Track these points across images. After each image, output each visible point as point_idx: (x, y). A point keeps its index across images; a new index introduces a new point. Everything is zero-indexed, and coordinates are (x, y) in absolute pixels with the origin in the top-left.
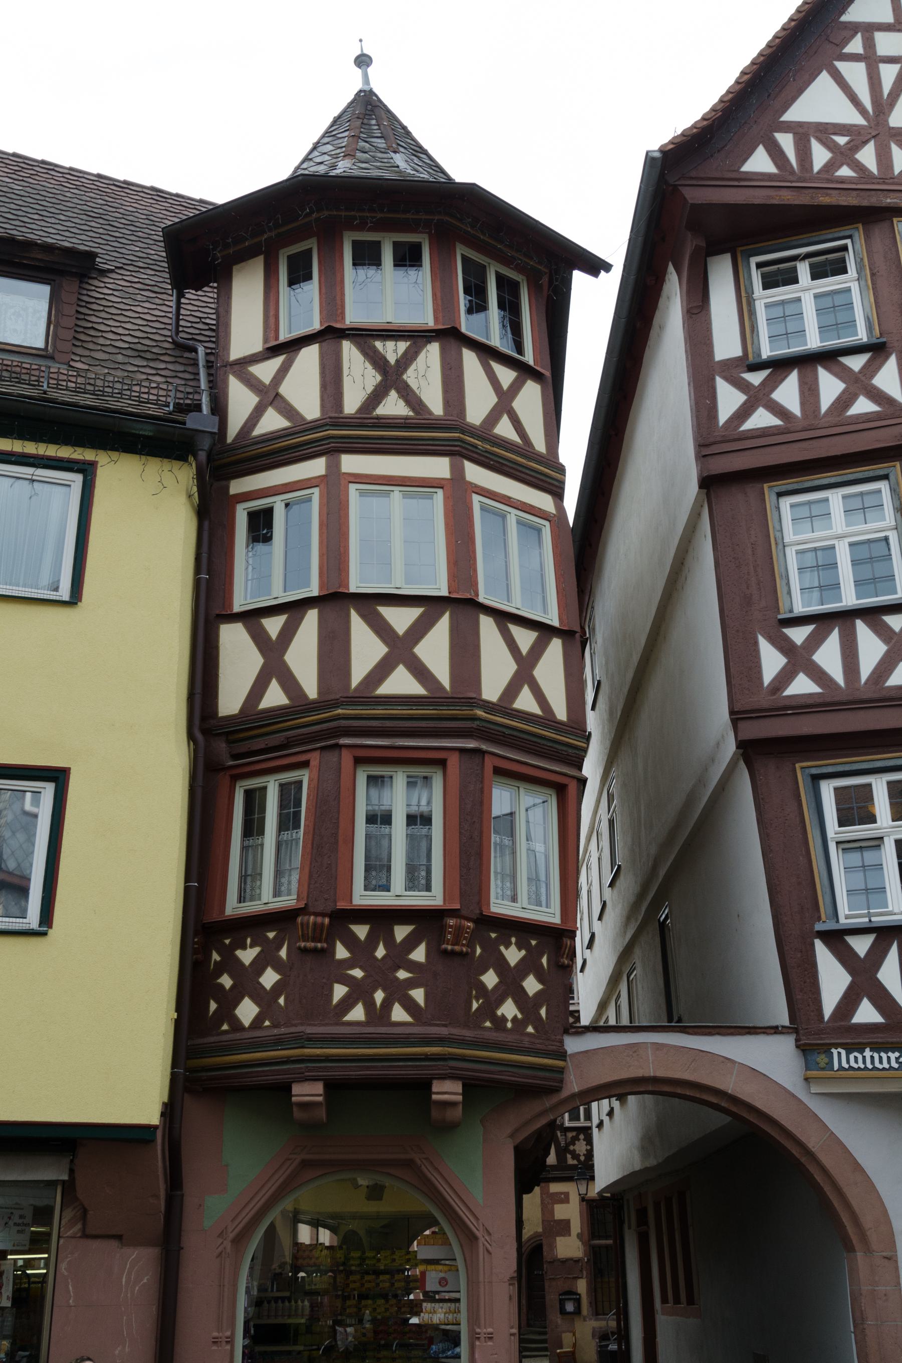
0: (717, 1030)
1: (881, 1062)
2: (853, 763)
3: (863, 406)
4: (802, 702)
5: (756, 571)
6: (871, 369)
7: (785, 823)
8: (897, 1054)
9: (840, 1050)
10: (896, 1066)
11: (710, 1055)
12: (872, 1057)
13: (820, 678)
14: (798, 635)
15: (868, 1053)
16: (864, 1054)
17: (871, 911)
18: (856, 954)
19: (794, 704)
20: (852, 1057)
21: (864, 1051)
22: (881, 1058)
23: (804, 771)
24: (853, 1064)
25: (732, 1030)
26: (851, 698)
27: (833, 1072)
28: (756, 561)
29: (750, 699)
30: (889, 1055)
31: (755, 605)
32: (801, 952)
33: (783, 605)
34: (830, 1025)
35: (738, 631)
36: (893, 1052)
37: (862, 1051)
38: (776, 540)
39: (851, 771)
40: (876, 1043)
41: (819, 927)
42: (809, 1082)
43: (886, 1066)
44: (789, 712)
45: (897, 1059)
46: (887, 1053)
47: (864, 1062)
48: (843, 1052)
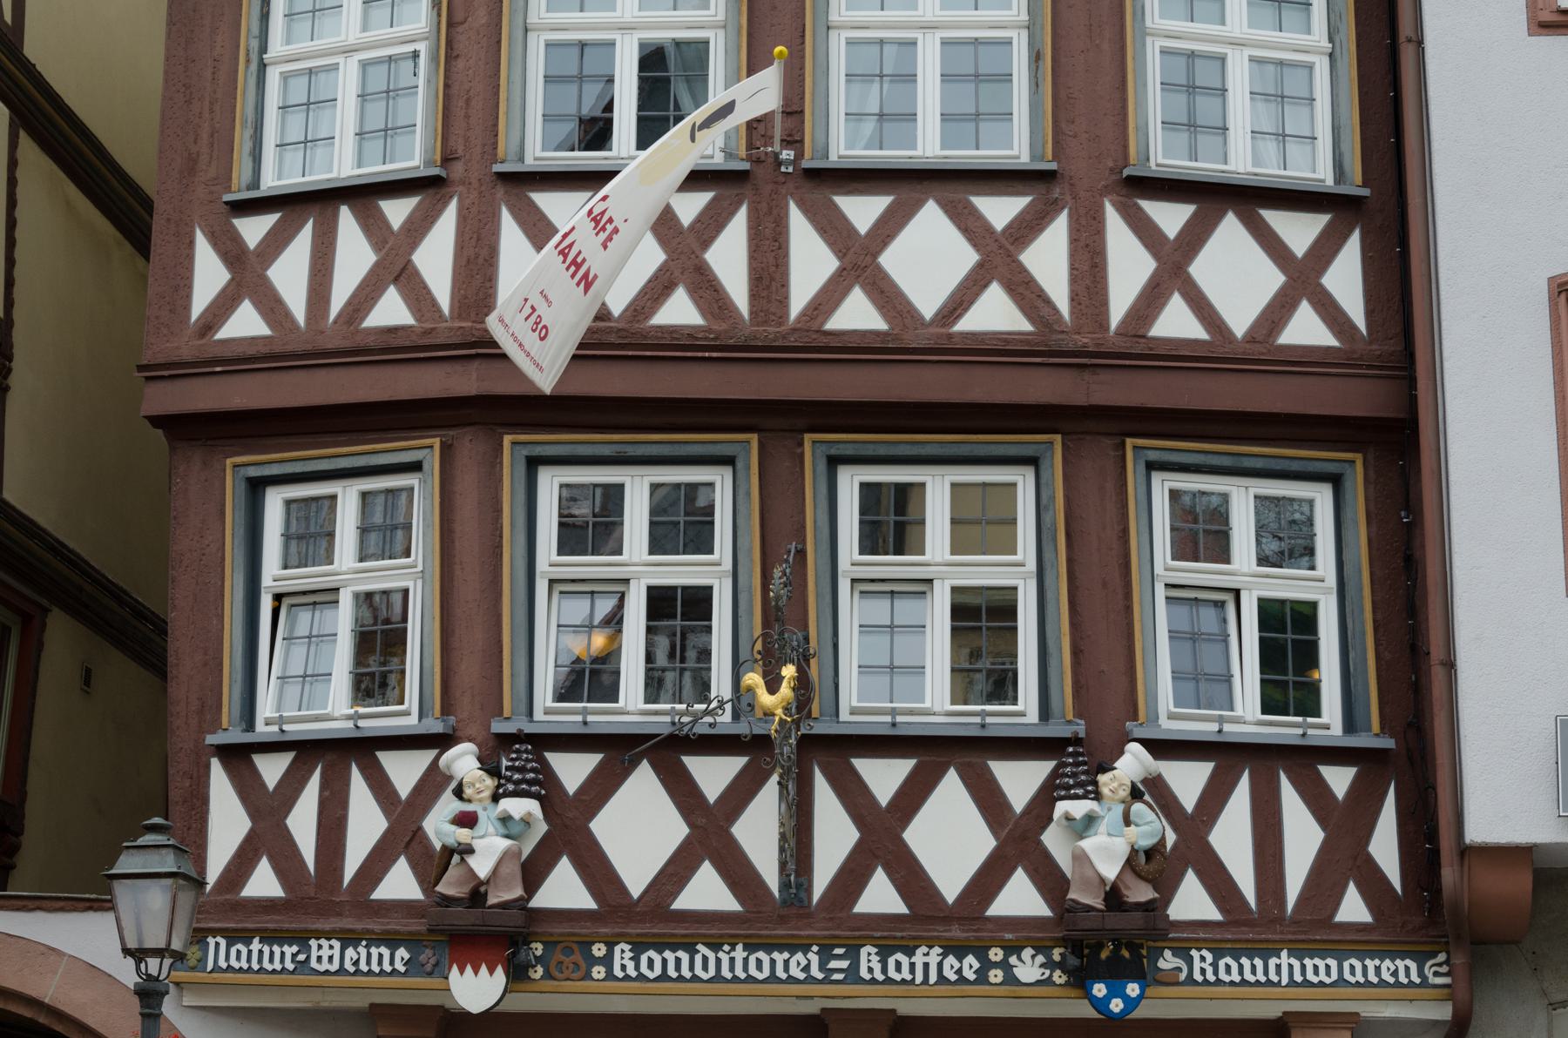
0: (37, 903)
1: (271, 960)
2: (333, 457)
4: (239, 351)
5: (212, 111)
7: (201, 560)
8: (295, 949)
9: (219, 939)
10: (290, 966)
11: (24, 942)
12: (261, 952)
13: (272, 309)
14: (253, 230)
15: (256, 945)
16: (251, 948)
17: (285, 714)
18: (263, 785)
19: (228, 354)
20: (233, 951)
21: (251, 943)
22: (272, 953)
23: (238, 472)
24: (234, 963)
25: (61, 904)
26: (309, 347)
27: (205, 975)
28: (215, 92)
29: (168, 345)
30: (283, 949)
31: (201, 174)
32: (191, 778)
33: (241, 171)
34: (212, 898)
35: (169, 220)
36: (290, 946)
37: (248, 942)
38: (248, 55)
39: (303, 473)
40: (266, 930)
41: (212, 739)
42: (182, 989)
43: (278, 967)
44: (218, 369)
45: (294, 956)
46: (281, 946)
47: (249, 960)
48: (223, 942)
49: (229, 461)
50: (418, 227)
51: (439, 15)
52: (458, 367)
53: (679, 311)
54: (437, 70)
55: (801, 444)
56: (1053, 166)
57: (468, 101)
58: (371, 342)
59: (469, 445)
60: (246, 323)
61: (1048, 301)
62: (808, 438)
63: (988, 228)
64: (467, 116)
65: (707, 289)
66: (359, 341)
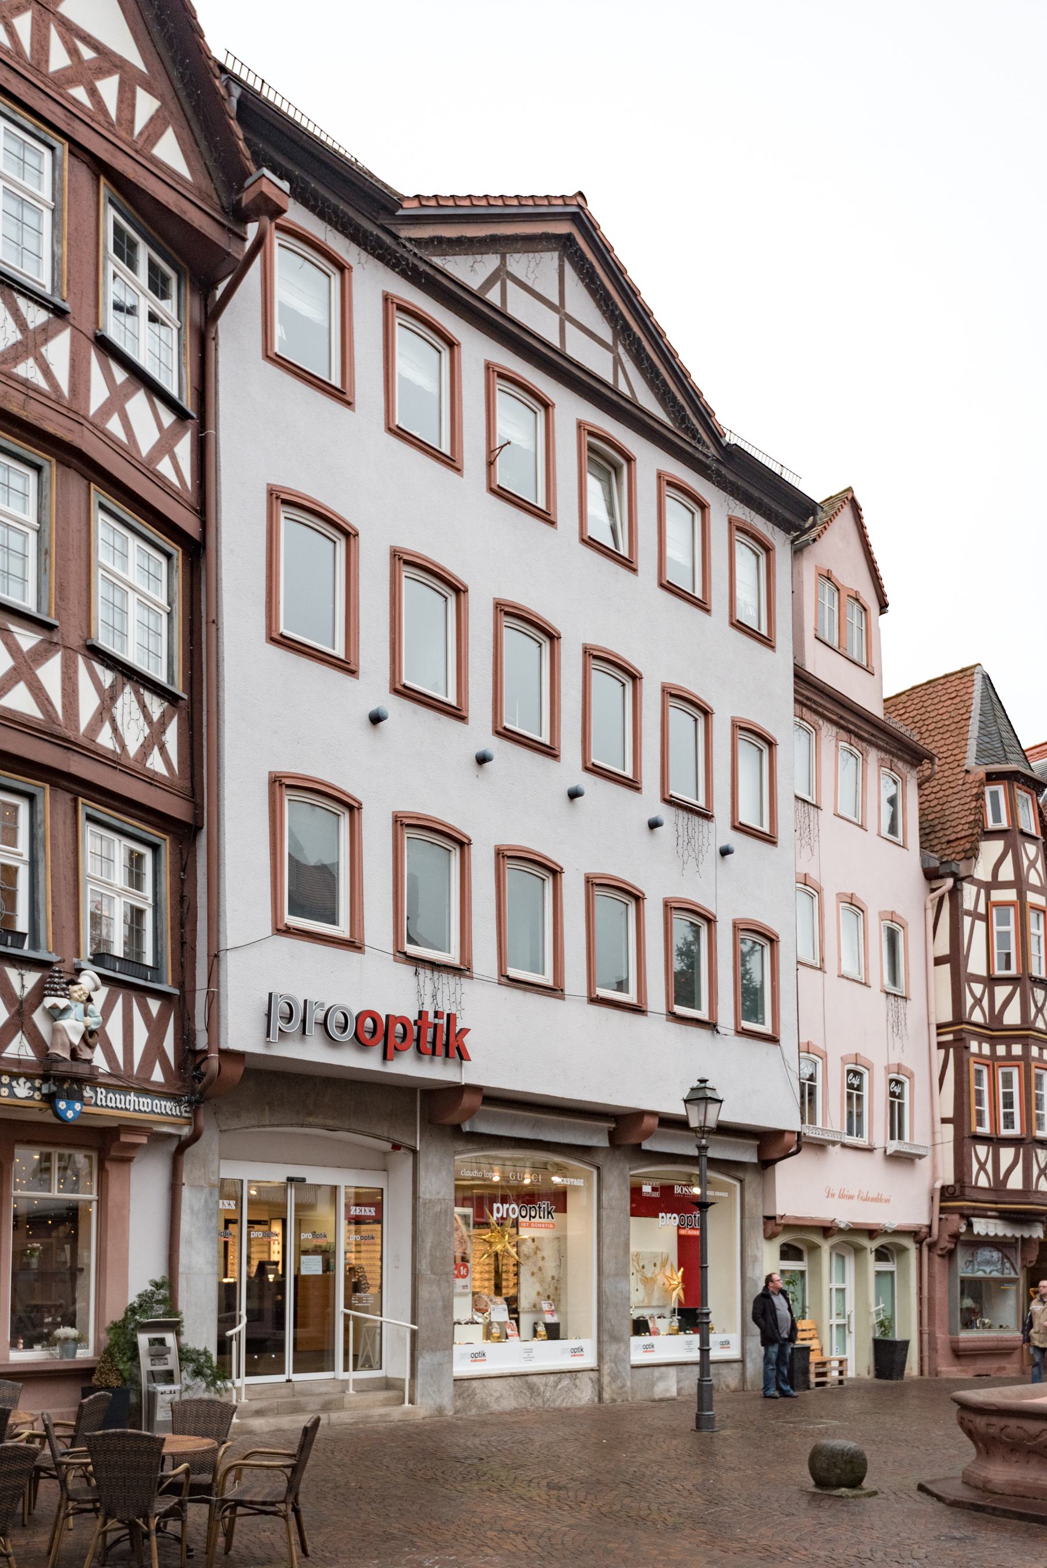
56: (56, 623)
61: (51, 704)
63: (19, 648)
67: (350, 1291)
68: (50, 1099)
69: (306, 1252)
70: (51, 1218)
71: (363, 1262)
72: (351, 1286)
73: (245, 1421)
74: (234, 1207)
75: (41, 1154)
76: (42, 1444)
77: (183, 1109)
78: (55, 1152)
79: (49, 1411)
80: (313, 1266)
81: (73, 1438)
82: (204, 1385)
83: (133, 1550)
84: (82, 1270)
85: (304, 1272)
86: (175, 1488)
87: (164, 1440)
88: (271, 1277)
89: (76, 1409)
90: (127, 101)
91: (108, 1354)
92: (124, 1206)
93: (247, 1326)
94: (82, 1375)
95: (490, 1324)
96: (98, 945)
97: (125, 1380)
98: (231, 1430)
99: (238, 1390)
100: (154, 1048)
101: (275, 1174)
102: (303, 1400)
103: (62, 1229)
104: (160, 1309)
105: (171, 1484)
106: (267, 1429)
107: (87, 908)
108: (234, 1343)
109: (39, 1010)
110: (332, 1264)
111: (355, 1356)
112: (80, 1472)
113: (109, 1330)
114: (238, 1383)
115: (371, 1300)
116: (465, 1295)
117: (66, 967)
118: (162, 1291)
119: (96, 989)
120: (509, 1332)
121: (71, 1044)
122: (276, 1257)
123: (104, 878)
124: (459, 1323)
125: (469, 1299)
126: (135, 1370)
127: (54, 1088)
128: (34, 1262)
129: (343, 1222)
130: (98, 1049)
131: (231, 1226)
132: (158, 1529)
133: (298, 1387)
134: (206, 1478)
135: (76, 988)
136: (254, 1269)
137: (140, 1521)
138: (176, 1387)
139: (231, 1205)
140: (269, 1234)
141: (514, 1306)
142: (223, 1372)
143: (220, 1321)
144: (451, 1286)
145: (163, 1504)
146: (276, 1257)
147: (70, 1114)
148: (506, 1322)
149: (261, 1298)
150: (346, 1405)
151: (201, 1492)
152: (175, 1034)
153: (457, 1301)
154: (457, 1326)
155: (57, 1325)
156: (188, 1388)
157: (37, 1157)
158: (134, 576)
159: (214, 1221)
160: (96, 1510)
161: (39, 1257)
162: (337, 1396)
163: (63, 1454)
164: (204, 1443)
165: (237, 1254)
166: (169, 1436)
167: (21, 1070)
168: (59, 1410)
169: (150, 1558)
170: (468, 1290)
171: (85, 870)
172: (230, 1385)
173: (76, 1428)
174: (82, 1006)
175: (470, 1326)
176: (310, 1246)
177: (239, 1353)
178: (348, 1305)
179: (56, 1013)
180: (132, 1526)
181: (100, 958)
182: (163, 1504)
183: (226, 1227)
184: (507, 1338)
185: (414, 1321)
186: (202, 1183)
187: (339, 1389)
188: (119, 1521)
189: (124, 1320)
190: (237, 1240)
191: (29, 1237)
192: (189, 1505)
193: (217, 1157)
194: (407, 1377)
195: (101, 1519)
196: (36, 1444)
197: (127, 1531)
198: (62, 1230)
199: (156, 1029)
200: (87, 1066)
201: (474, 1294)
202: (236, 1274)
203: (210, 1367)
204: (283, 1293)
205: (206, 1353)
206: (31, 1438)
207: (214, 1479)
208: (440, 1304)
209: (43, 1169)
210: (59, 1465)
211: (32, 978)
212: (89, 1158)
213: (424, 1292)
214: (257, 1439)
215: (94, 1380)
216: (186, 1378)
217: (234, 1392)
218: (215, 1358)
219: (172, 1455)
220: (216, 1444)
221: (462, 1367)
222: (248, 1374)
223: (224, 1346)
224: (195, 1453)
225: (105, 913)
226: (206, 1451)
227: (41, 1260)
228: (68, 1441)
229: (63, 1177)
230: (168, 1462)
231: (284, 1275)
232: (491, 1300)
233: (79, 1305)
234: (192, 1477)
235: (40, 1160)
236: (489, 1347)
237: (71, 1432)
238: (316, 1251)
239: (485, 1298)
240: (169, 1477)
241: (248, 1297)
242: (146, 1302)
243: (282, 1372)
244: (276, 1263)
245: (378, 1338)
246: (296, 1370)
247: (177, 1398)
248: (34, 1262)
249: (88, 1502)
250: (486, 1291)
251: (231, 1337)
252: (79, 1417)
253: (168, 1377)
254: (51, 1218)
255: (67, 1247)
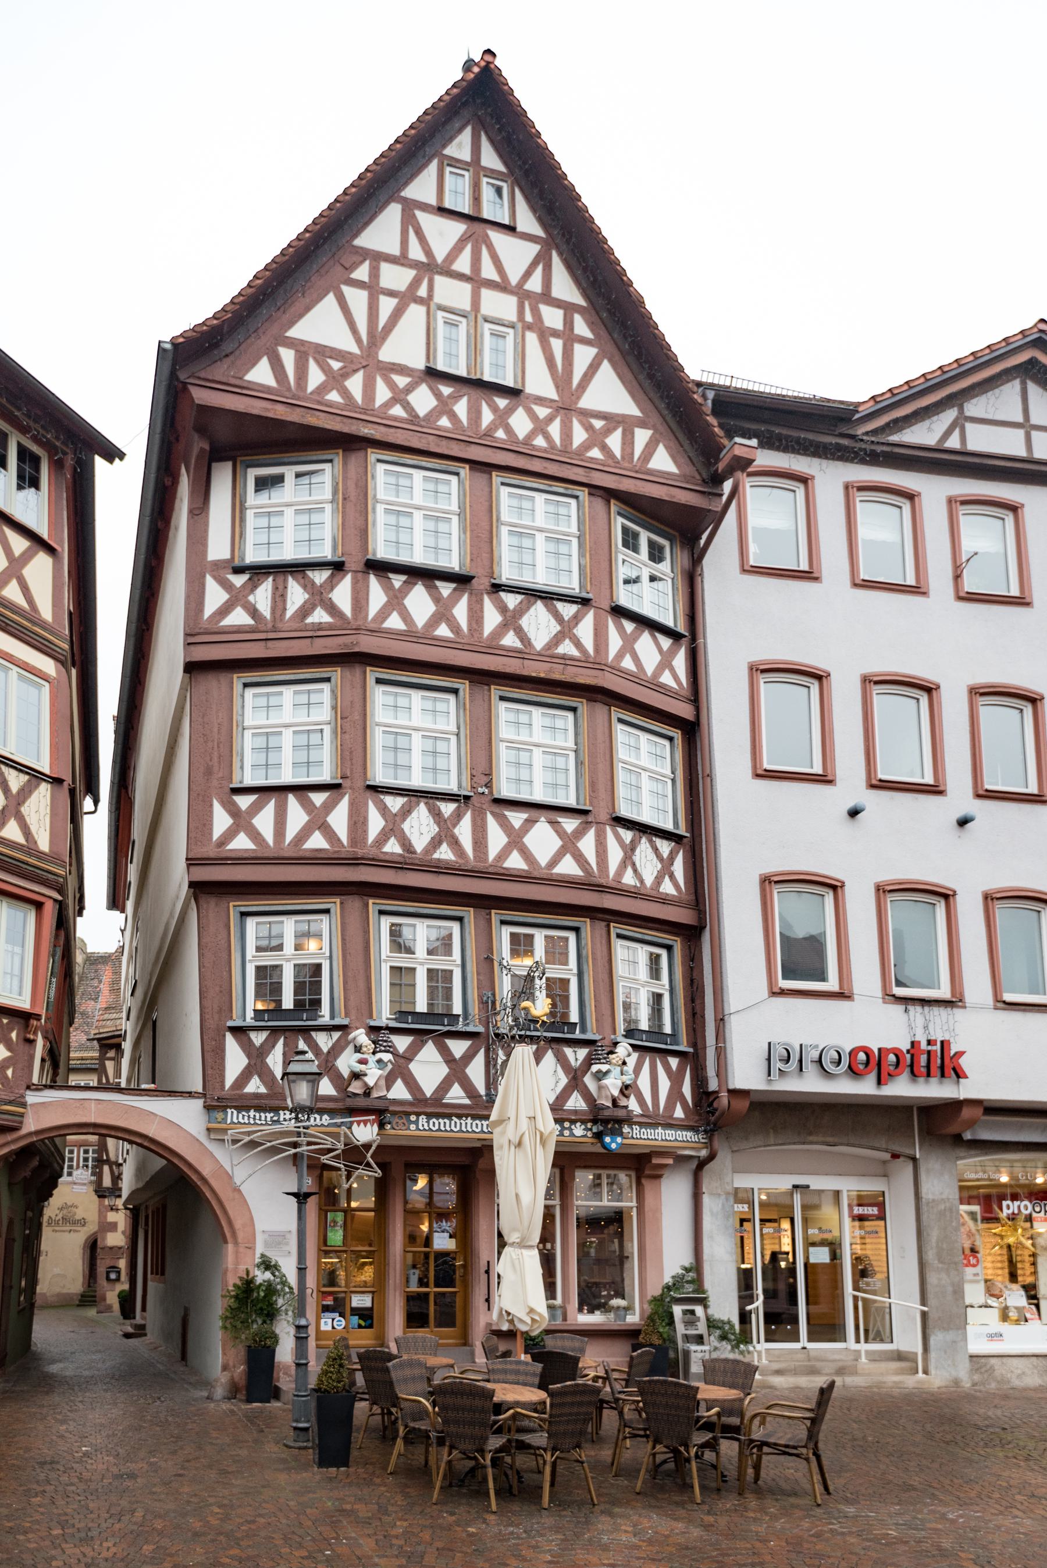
3: (320, 616)
6: (331, 584)
26: (276, 855)
49: (231, 904)
50: (329, 807)
51: (336, 713)
52: (351, 868)
53: (445, 853)
54: (336, 737)
55: (490, 914)
57: (351, 753)
58: (308, 855)
59: (354, 903)
60: (242, 843)
61: (589, 864)
62: (493, 911)
64: (351, 760)
65: (455, 844)
66: (301, 854)
67: (858, 1277)
68: (599, 1136)
69: (813, 1244)
70: (603, 1220)
71: (868, 1252)
72: (858, 1273)
73: (765, 1378)
74: (747, 1210)
75: (594, 1175)
76: (604, 1383)
77: (700, 1137)
78: (604, 1173)
79: (606, 1359)
80: (821, 1256)
81: (627, 1381)
82: (729, 1347)
83: (677, 1470)
84: (627, 1257)
85: (812, 1260)
86: (709, 1426)
87: (698, 1388)
88: (783, 1264)
89: (628, 1359)
90: (628, 441)
91: (651, 1320)
92: (658, 1210)
93: (765, 1303)
94: (631, 1335)
95: (1006, 1308)
96: (629, 1022)
97: (664, 1340)
98: (754, 1384)
99: (759, 1353)
100: (675, 1093)
101: (782, 1183)
102: (818, 1364)
103: (611, 1227)
104: (690, 1288)
105: (705, 1422)
106: (785, 1386)
107: (620, 999)
108: (753, 1316)
109: (589, 1073)
110: (838, 1254)
111: (866, 1331)
112: (633, 1407)
113: (650, 1302)
114: (759, 1347)
115: (879, 1285)
116: (977, 1282)
117: (606, 1042)
118: (691, 1274)
119: (629, 1055)
120: (1028, 1315)
121: (612, 1096)
122: (787, 1247)
123: (631, 976)
124: (972, 1307)
125: (981, 1287)
126: (672, 1333)
127: (601, 1128)
128: (593, 1252)
129: (847, 1220)
130: (632, 1098)
131: (745, 1224)
132: (697, 1456)
133: (812, 1354)
134: (735, 1421)
135: (614, 1056)
136: (767, 1258)
137: (682, 1449)
138: (706, 1348)
139: (745, 1208)
140: (779, 1230)
141: (1033, 1293)
142: (745, 1337)
143: (740, 1297)
144: (961, 1275)
145: (700, 1438)
146: (787, 1247)
147: (614, 1146)
148: (1024, 1307)
149: (775, 1280)
150: (859, 1371)
151: (732, 1431)
152: (692, 1084)
153: (968, 1288)
154: (969, 1310)
155: (611, 1297)
156: (716, 1349)
157: (591, 1177)
158: (645, 761)
159: (731, 1220)
160: (647, 1436)
161: (596, 1248)
162: (849, 1363)
163: (620, 1392)
164: (732, 1394)
165: (752, 1245)
166: (700, 1385)
167: (578, 1117)
168: (614, 1359)
169: (692, 1478)
170: (981, 1277)
171: (617, 972)
172: (751, 1348)
173: (629, 1374)
174: (618, 1069)
175: (983, 1309)
176: (817, 1239)
177: (759, 1323)
178: (856, 1288)
179: (601, 1075)
180: (676, 1452)
181: (630, 1033)
182: (700, 1438)
183: (741, 1225)
184: (1026, 1321)
185: (923, 1303)
186: (719, 1191)
187: (852, 1357)
188: (665, 1447)
189: (662, 1295)
190: (751, 1235)
191: (588, 1234)
192: (722, 1440)
193: (730, 1172)
194: (919, 1350)
195: (651, 1444)
196: (600, 1384)
197: (671, 1455)
198: (612, 1229)
199: (676, 1080)
200: (624, 1110)
201: (986, 1281)
202: (752, 1261)
203: (734, 1334)
204: (795, 1277)
205: (729, 1322)
206: (596, 1379)
207: (742, 1422)
208: (950, 1289)
209: (596, 1185)
210: (617, 1400)
211: (583, 1053)
212: (629, 1176)
213: (932, 1279)
214: (778, 1393)
215: (641, 1339)
216: (714, 1341)
217: (756, 1355)
218: (737, 1327)
219: (705, 1400)
220: (742, 1395)
221: (977, 1345)
222: (767, 1340)
223: (744, 1318)
224: (725, 1401)
225: (633, 1000)
226: (734, 1400)
227: (597, 1252)
228: (623, 1383)
229: (610, 1191)
230: (703, 1405)
231: (794, 1262)
232: (1006, 1287)
233: (627, 1282)
234: (723, 1419)
235: (594, 1179)
236: (1006, 1328)
237: (625, 1376)
238: (823, 1243)
239: (1000, 1285)
240: (703, 1417)
241: (764, 1279)
242: (678, 1282)
243: (798, 1341)
244: (787, 1253)
245: (887, 1317)
246: (810, 1340)
247: (707, 1357)
248: (593, 1252)
249: (639, 1429)
250: (1000, 1278)
251: (750, 1312)
252: (630, 1366)
253: (699, 1339)
254: (603, 1220)
255: (616, 1241)
